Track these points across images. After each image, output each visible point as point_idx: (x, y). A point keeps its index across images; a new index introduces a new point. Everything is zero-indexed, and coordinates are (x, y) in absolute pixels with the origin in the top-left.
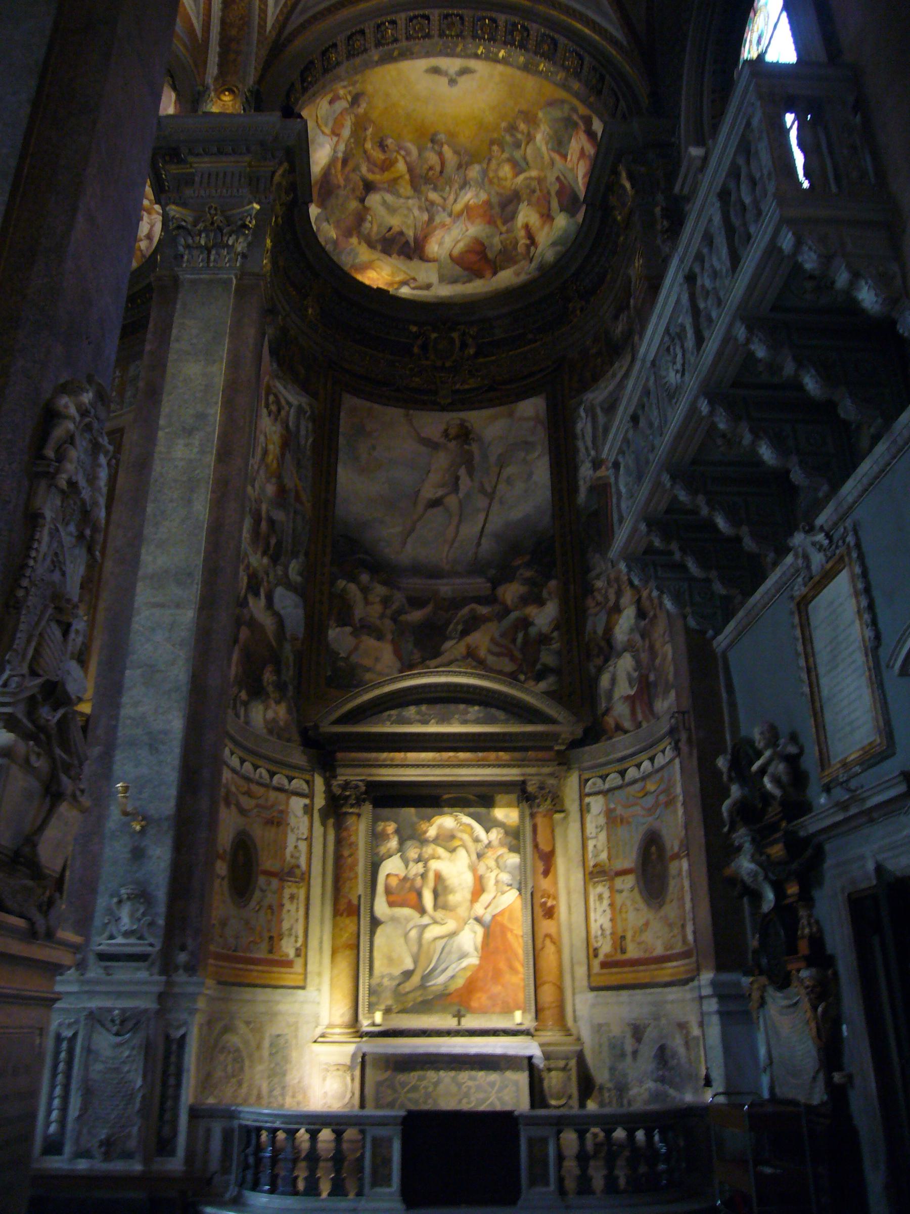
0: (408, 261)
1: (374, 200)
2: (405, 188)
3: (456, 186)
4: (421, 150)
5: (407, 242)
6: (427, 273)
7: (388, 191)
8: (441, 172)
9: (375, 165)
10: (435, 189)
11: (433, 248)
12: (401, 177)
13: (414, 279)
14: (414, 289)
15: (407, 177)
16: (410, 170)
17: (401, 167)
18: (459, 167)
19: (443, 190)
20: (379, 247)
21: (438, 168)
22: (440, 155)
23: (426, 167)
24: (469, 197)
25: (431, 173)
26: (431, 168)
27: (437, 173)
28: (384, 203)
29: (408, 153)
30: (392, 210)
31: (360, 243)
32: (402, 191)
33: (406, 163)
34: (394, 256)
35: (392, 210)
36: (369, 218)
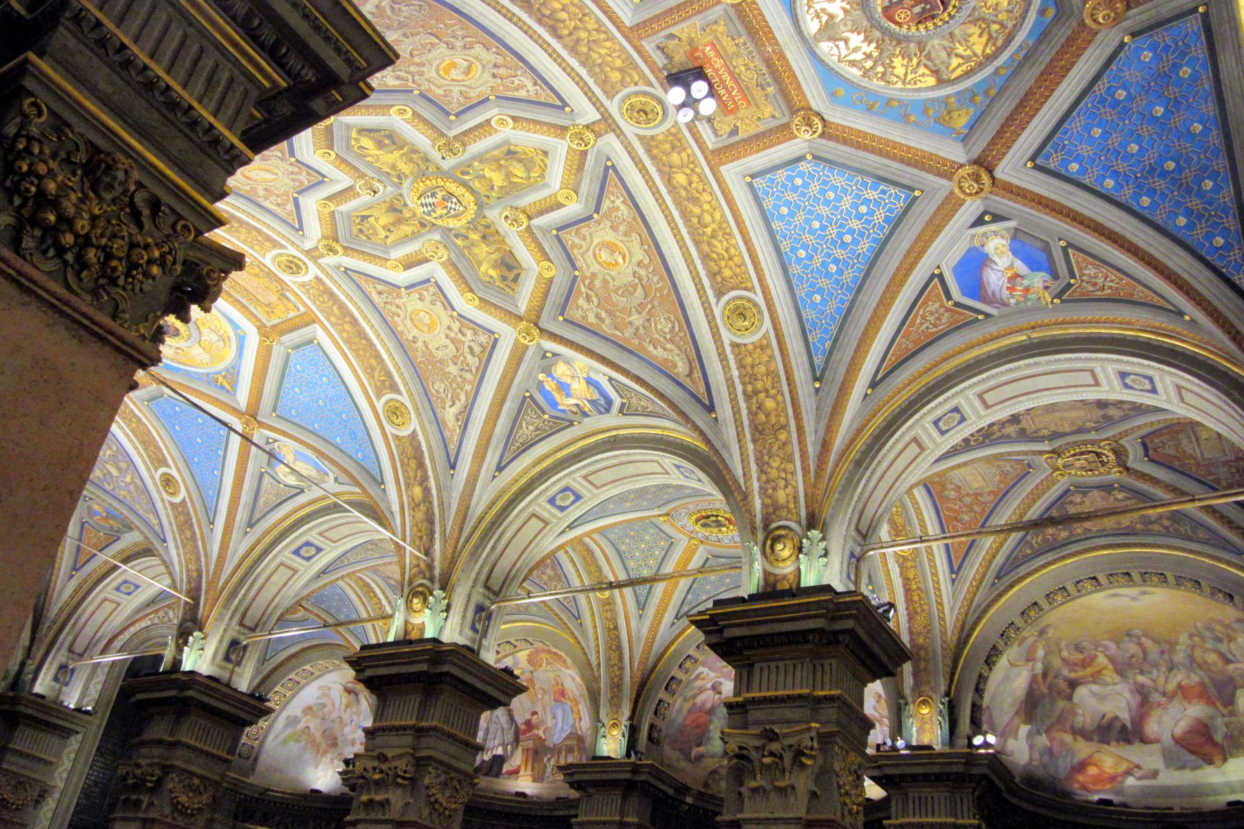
0: (1128, 747)
1: (1082, 692)
2: (1110, 675)
3: (1163, 669)
4: (1118, 644)
5: (1124, 726)
6: (1149, 758)
7: (1094, 682)
8: (1145, 658)
9: (1075, 665)
10: (1142, 673)
11: (1152, 727)
12: (1105, 668)
13: (1138, 767)
14: (1139, 779)
15: (1110, 667)
16: (1112, 660)
17: (1102, 660)
18: (1162, 653)
19: (1150, 673)
20: (1096, 738)
21: (1141, 656)
22: (1140, 644)
23: (1128, 655)
24: (1179, 677)
25: (1134, 660)
26: (1133, 656)
27: (1140, 660)
28: (1093, 693)
29: (1106, 648)
30: (1101, 698)
31: (1075, 740)
32: (1108, 679)
33: (1107, 656)
34: (1114, 743)
35: (1101, 698)
36: (1080, 711)
